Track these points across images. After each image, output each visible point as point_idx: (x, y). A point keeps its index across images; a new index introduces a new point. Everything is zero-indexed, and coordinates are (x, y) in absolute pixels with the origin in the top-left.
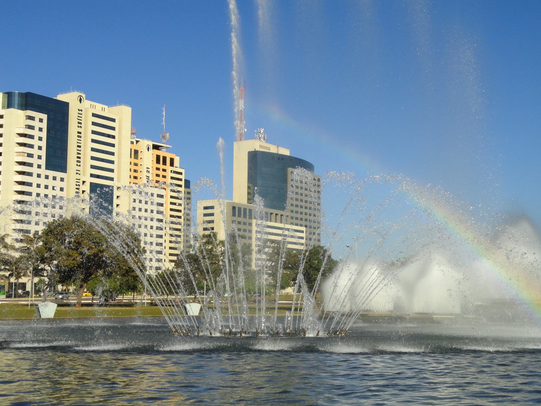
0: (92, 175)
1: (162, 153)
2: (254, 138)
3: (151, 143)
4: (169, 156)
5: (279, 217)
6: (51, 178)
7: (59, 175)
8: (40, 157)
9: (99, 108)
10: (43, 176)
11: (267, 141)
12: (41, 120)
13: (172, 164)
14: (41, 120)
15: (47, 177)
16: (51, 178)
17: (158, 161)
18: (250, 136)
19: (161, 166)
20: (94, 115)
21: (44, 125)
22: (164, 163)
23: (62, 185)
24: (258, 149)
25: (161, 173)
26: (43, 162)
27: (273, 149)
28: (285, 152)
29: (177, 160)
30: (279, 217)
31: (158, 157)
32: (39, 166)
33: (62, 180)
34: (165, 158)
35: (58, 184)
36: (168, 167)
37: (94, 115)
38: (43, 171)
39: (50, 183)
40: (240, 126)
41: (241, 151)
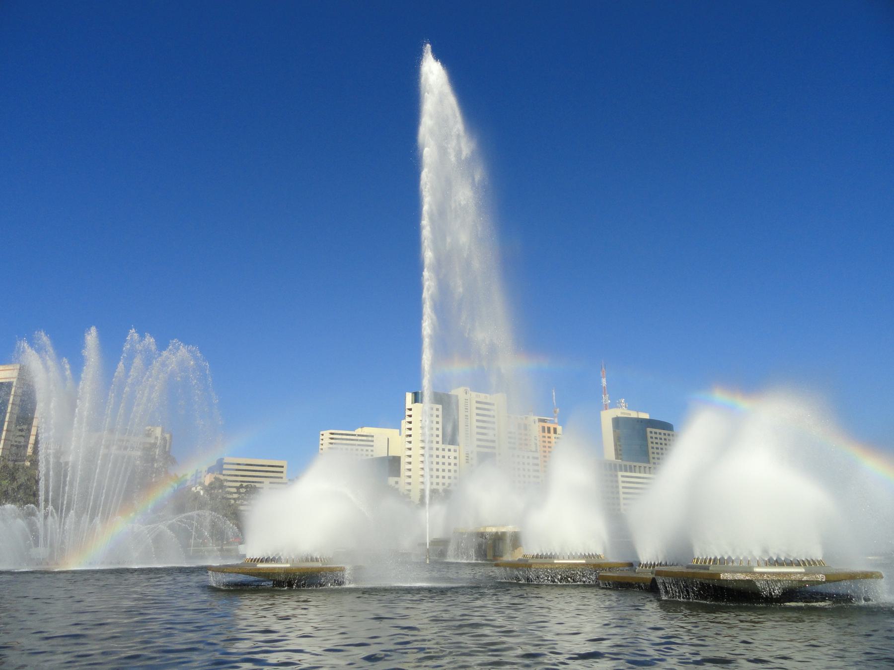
0: (478, 446)
1: (546, 425)
2: (617, 407)
3: (537, 418)
4: (552, 426)
5: (642, 469)
6: (446, 450)
7: (452, 447)
8: (438, 436)
9: (482, 397)
10: (441, 449)
11: (629, 409)
12: (437, 410)
13: (555, 432)
14: (437, 410)
15: (444, 450)
16: (446, 450)
17: (544, 431)
18: (613, 405)
19: (546, 434)
20: (477, 402)
21: (440, 413)
22: (549, 431)
23: (456, 454)
24: (620, 415)
25: (547, 440)
26: (440, 439)
27: (634, 415)
28: (645, 416)
29: (559, 428)
30: (642, 469)
31: (543, 428)
32: (438, 442)
33: (455, 451)
34: (549, 429)
35: (452, 454)
36: (552, 435)
37: (477, 402)
38: (441, 446)
39: (446, 453)
40: (606, 399)
41: (607, 417)
